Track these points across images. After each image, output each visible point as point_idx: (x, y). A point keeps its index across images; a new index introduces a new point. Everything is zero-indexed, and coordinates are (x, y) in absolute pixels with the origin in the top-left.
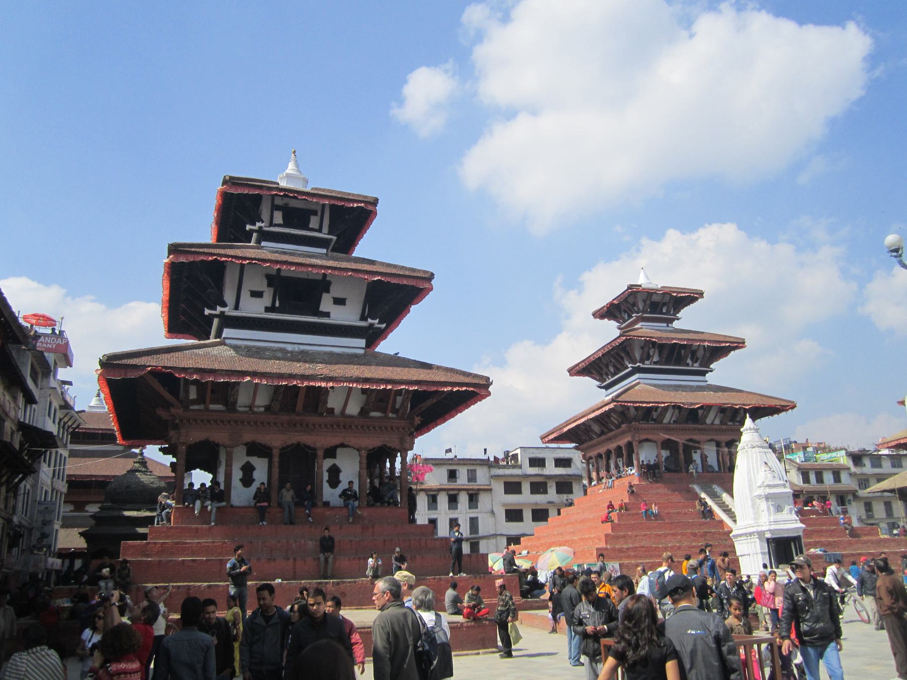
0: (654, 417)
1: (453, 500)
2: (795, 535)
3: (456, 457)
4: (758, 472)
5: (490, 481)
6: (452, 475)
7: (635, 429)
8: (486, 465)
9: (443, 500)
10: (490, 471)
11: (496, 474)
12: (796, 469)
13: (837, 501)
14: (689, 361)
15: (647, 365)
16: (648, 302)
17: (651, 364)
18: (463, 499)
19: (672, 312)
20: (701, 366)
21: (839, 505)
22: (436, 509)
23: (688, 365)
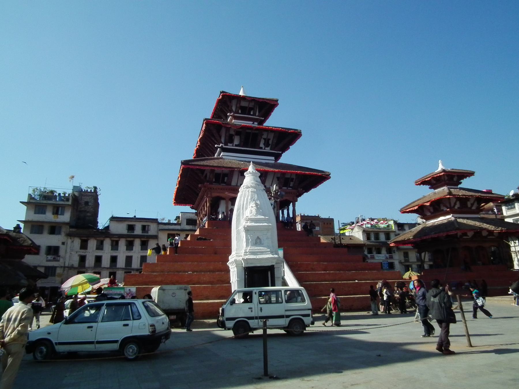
0: (225, 181)
1: (130, 246)
2: (269, 264)
3: (135, 216)
4: (246, 209)
5: (158, 233)
6: (131, 228)
7: (208, 188)
8: (156, 222)
9: (122, 244)
10: (158, 226)
11: (163, 229)
12: (362, 231)
13: (387, 251)
14: (262, 145)
15: (230, 146)
16: (238, 105)
17: (233, 146)
18: (137, 243)
19: (257, 114)
20: (271, 149)
21: (387, 254)
22: (117, 250)
23: (261, 148)
